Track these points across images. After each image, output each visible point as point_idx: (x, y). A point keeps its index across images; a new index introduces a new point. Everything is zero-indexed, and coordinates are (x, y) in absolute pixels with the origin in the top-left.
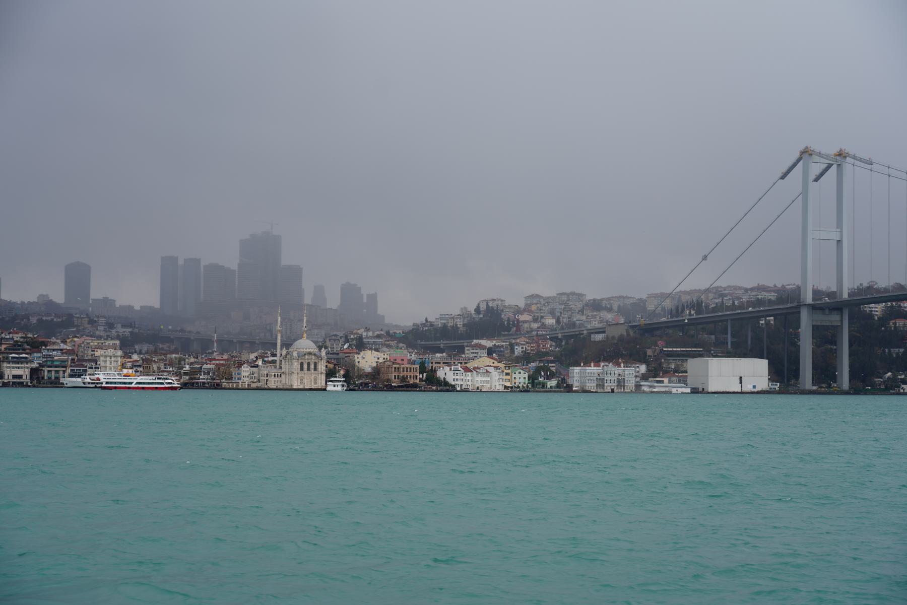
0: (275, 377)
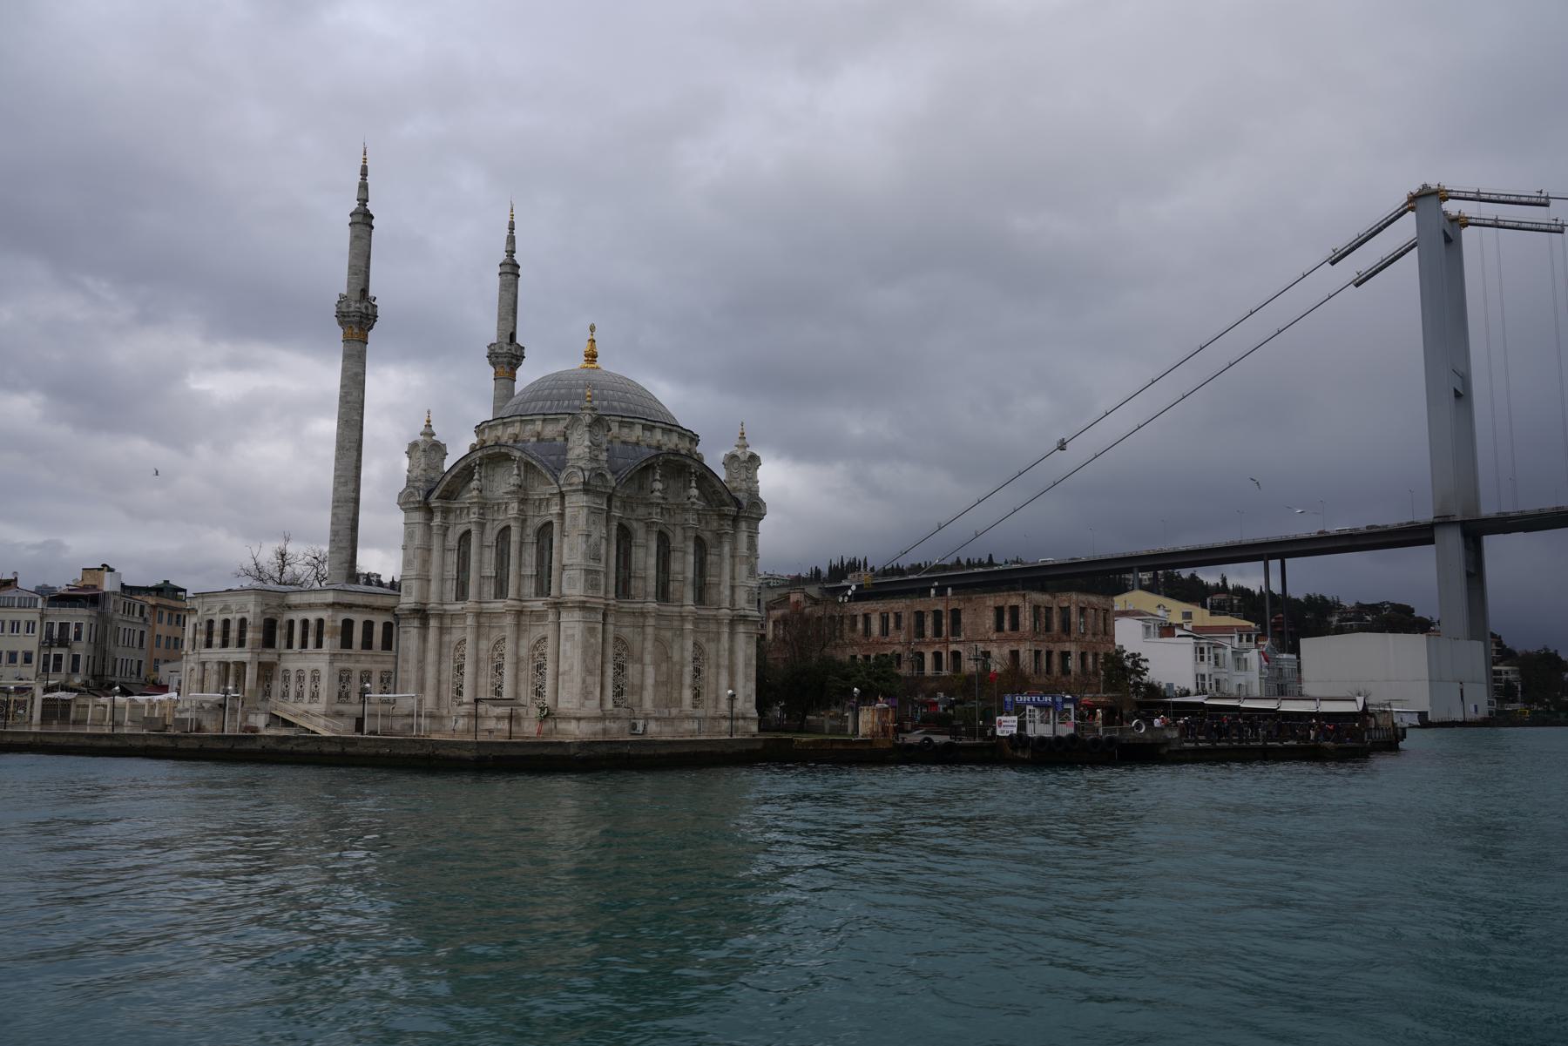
0: (347, 642)
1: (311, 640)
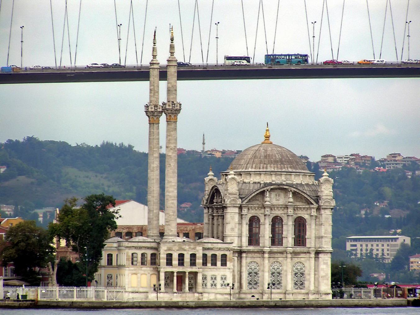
1: (219, 263)
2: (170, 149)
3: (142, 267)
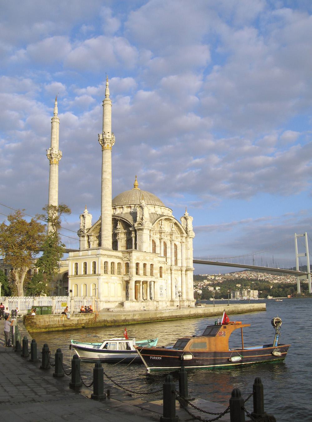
2: (108, 173)
3: (112, 276)
